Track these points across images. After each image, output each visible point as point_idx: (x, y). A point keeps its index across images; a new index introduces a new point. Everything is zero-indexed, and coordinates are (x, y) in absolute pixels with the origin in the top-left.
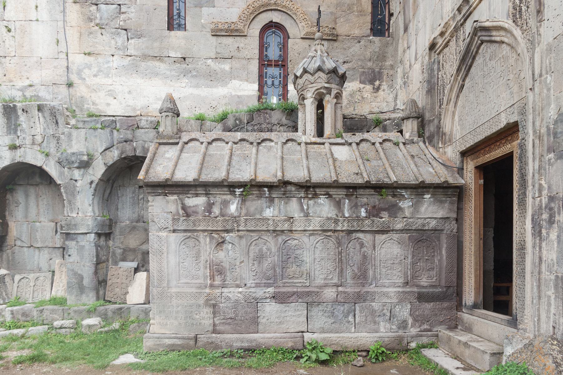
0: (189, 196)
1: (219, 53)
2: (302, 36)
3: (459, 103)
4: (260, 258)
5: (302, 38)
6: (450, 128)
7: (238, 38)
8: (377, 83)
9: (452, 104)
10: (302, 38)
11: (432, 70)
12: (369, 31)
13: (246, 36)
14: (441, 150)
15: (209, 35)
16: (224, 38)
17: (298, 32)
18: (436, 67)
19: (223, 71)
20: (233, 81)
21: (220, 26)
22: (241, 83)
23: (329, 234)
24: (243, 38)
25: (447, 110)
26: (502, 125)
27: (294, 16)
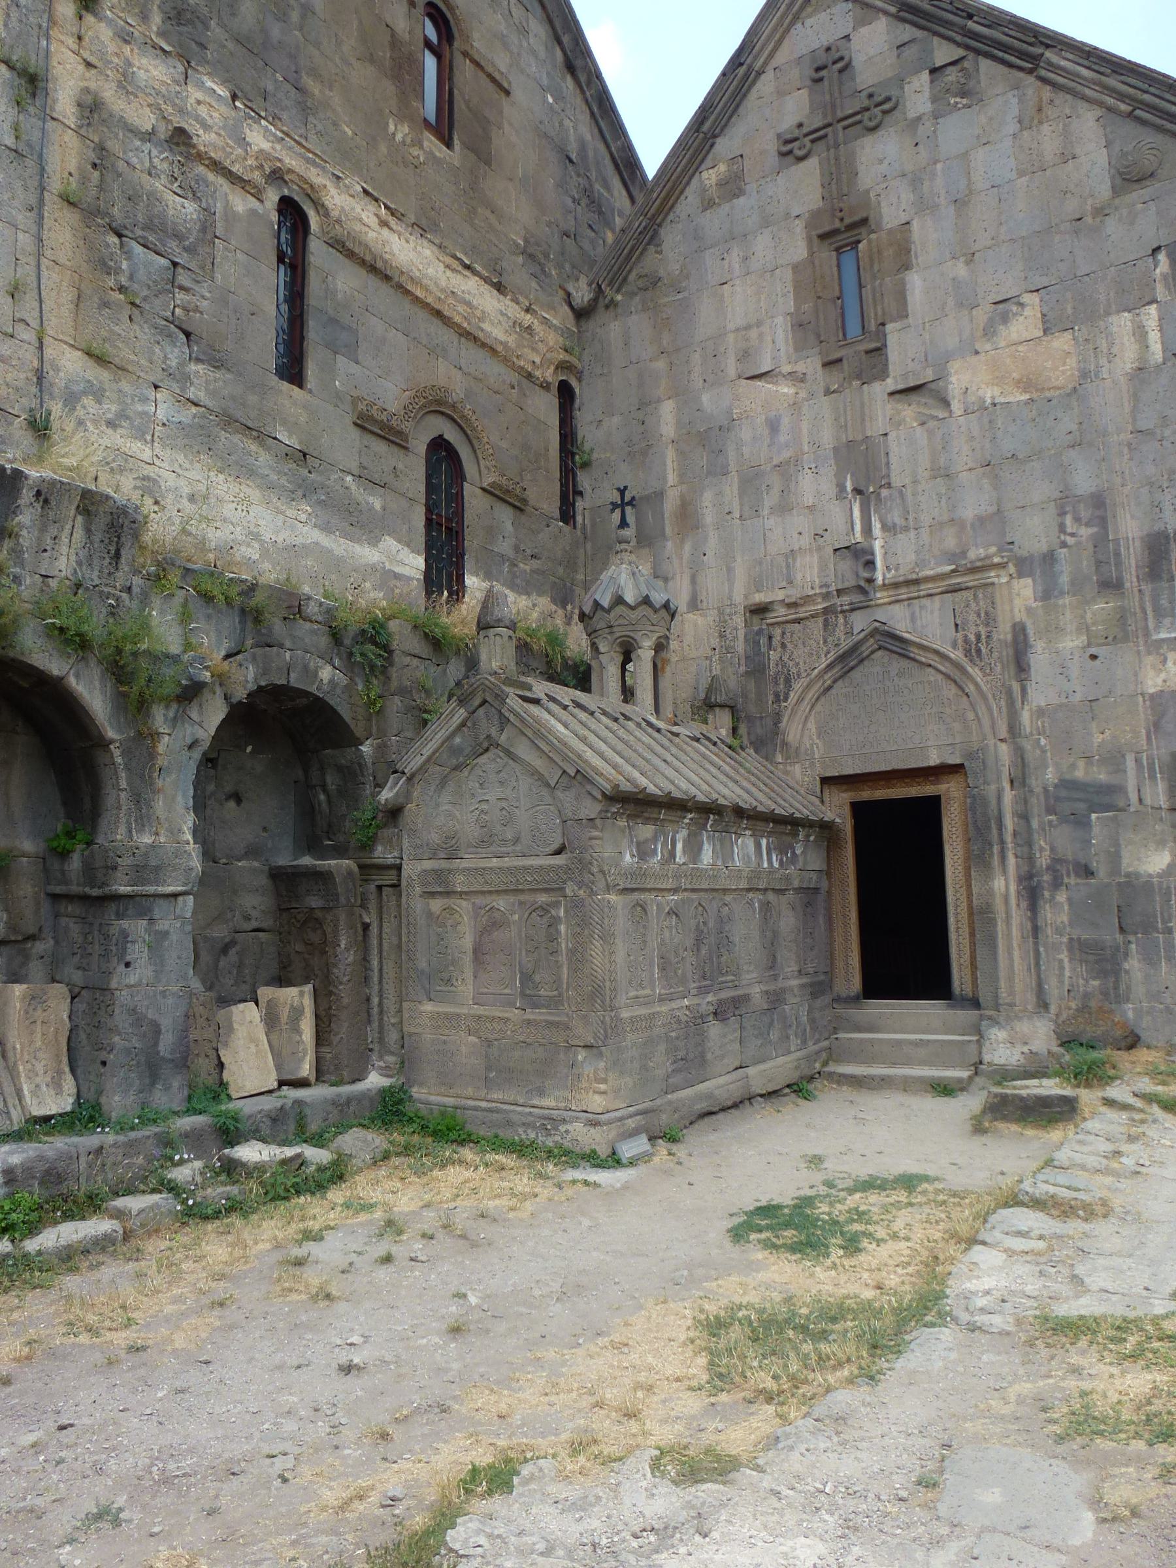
0: (639, 821)
1: (365, 468)
2: (485, 485)
3: (818, 708)
4: (698, 942)
5: (483, 489)
6: (798, 736)
7: (395, 449)
8: (569, 607)
9: (805, 706)
10: (483, 489)
11: (757, 644)
12: (557, 514)
13: (406, 448)
14: (781, 766)
15: (348, 420)
16: (373, 438)
17: (477, 474)
18: (763, 641)
19: (371, 509)
20: (387, 538)
21: (374, 412)
22: (400, 547)
23: (751, 895)
24: (403, 451)
25: (793, 712)
26: (932, 763)
27: (475, 442)
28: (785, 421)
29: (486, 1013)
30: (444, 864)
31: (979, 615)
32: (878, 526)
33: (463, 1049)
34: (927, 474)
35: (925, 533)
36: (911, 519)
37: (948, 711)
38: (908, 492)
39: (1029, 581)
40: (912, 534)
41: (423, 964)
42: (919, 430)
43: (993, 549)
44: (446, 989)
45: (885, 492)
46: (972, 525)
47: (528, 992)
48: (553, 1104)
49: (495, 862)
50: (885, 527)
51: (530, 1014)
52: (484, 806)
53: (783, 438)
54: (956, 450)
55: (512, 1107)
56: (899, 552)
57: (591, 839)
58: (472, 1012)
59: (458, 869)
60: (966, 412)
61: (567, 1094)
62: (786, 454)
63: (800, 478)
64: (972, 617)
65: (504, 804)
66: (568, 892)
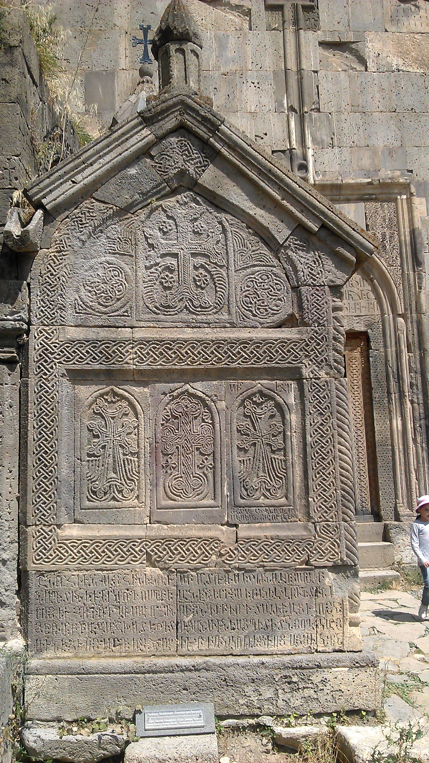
28: (232, 41)
29: (176, 533)
30: (103, 333)
31: (384, 220)
32: (310, 139)
33: (138, 587)
34: (349, 108)
35: (346, 152)
36: (335, 139)
37: (355, 290)
38: (334, 117)
39: (424, 200)
40: (336, 150)
41: (64, 471)
42: (343, 74)
43: (398, 173)
44: (104, 504)
45: (315, 115)
46: (383, 152)
47: (242, 501)
48: (288, 647)
49: (189, 334)
50: (314, 140)
51: (244, 531)
52: (171, 261)
53: (230, 54)
54: (371, 96)
55: (231, 660)
56: (326, 162)
57: (336, 309)
58: (153, 533)
59: (133, 341)
60: (378, 71)
61: (308, 631)
62: (232, 67)
63: (244, 88)
64: (379, 221)
65: (201, 261)
66: (306, 372)
